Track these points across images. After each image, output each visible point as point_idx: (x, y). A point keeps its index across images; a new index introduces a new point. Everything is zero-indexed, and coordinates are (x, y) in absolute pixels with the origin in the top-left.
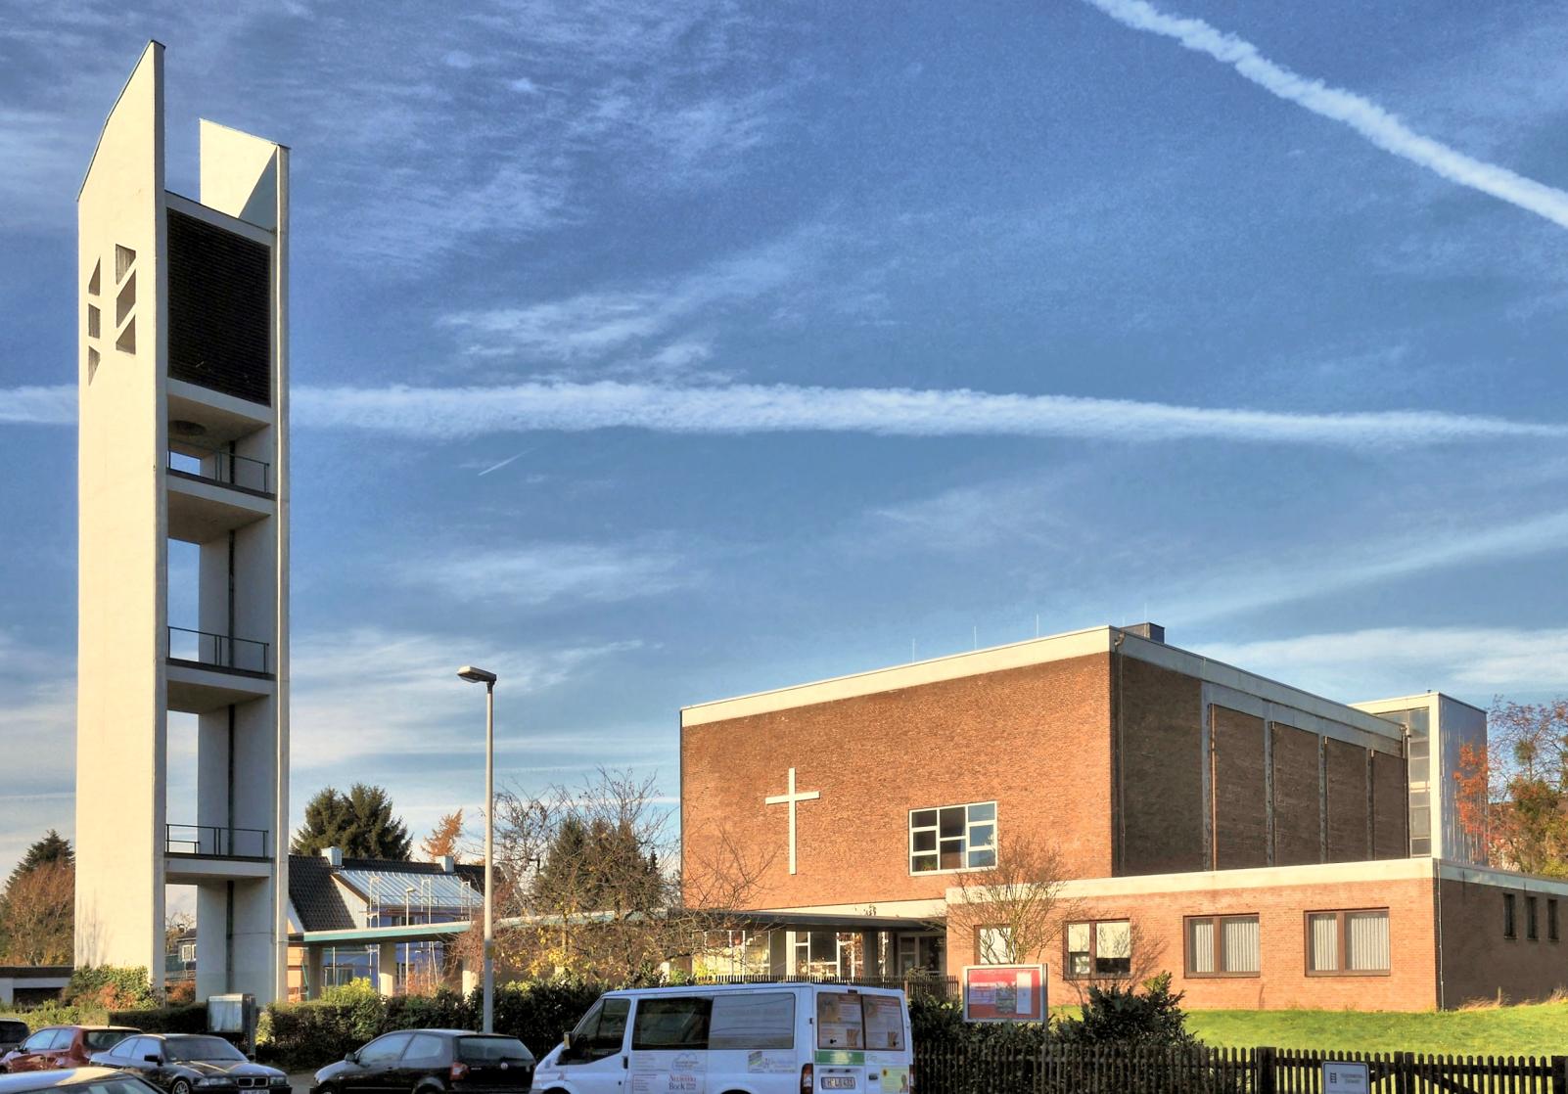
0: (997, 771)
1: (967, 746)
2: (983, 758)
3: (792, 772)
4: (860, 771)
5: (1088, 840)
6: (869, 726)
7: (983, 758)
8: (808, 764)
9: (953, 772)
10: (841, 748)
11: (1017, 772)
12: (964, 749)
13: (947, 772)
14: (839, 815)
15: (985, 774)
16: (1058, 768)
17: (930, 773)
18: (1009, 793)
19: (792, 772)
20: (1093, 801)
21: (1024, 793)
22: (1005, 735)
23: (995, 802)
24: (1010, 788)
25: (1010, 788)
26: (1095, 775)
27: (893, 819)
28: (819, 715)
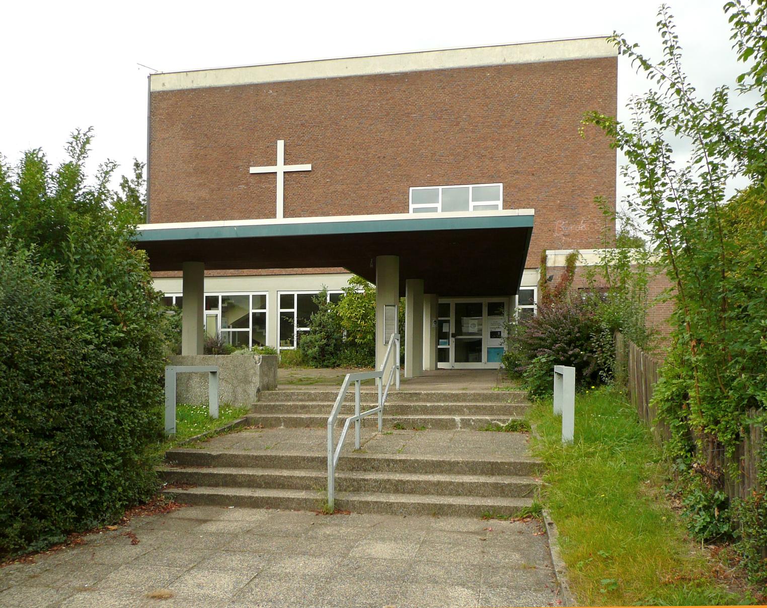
0: (504, 157)
1: (473, 132)
2: (489, 143)
3: (281, 144)
4: (357, 147)
5: (594, 224)
6: (368, 105)
7: (489, 143)
8: (299, 137)
9: (458, 154)
10: (337, 124)
11: (524, 158)
12: (470, 134)
13: (452, 154)
14: (332, 189)
15: (492, 158)
16: (566, 157)
17: (434, 154)
18: (516, 176)
19: (281, 144)
20: (600, 188)
21: (531, 178)
22: (513, 124)
23: (501, 185)
24: (517, 172)
25: (517, 172)
26: (602, 166)
27: (391, 195)
28: (312, 91)
